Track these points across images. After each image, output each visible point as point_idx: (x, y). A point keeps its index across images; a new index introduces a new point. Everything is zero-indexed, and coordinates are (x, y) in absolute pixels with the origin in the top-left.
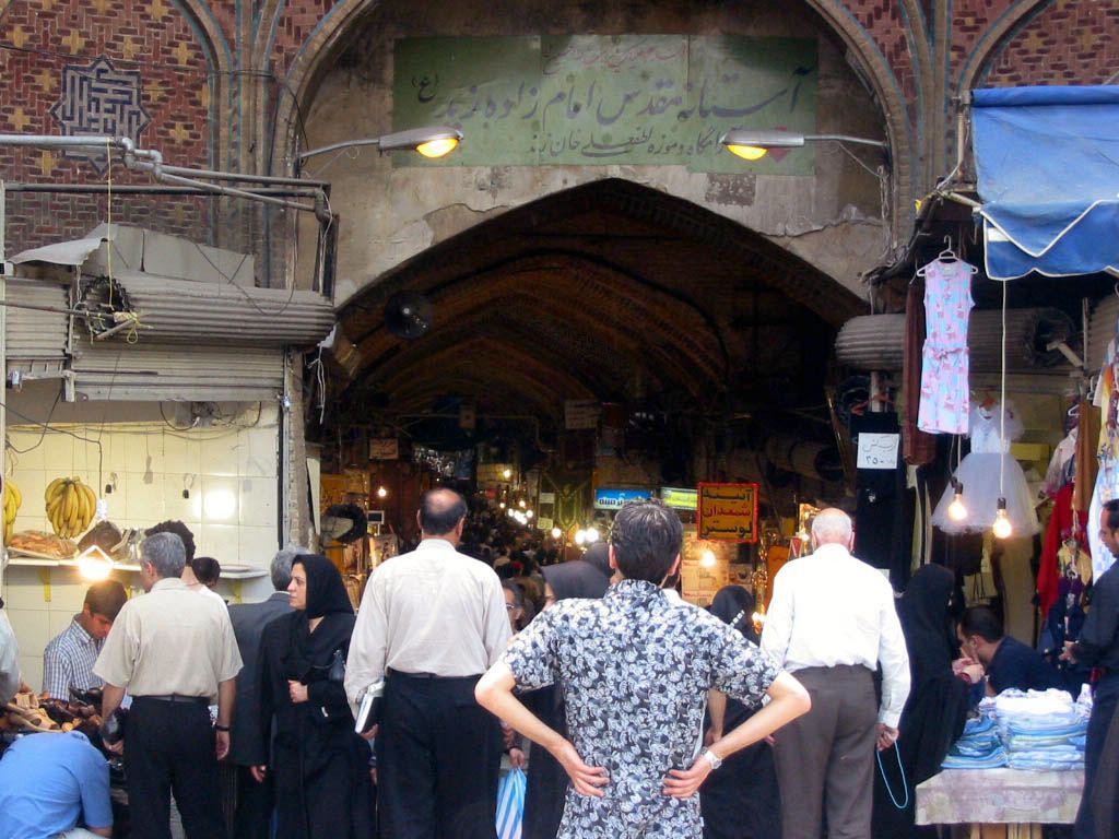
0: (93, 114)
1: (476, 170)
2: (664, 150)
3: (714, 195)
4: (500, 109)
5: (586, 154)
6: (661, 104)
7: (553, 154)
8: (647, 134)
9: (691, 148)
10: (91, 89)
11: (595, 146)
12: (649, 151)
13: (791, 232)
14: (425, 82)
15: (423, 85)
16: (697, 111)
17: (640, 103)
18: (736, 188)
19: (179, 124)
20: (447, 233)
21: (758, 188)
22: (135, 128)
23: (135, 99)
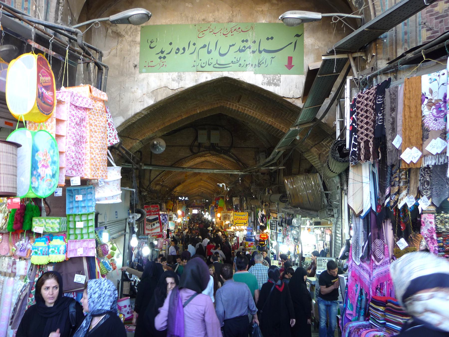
1: (171, 73)
2: (245, 66)
3: (265, 83)
4: (181, 51)
5: (214, 67)
6: (243, 49)
7: (202, 67)
8: (238, 60)
9: (256, 65)
11: (219, 64)
12: (239, 66)
13: (295, 97)
14: (152, 41)
15: (151, 42)
16: (258, 51)
17: (236, 48)
18: (273, 81)
20: (161, 97)
21: (281, 80)
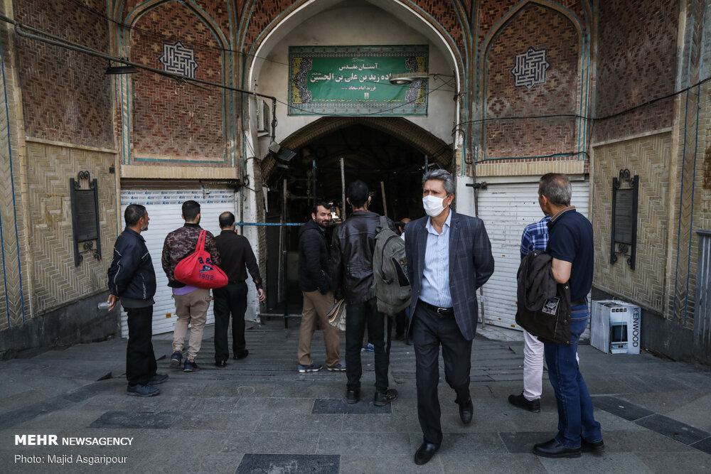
0: (176, 61)
10: (174, 53)
19: (210, 69)
22: (193, 69)
23: (192, 58)
